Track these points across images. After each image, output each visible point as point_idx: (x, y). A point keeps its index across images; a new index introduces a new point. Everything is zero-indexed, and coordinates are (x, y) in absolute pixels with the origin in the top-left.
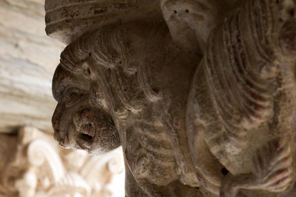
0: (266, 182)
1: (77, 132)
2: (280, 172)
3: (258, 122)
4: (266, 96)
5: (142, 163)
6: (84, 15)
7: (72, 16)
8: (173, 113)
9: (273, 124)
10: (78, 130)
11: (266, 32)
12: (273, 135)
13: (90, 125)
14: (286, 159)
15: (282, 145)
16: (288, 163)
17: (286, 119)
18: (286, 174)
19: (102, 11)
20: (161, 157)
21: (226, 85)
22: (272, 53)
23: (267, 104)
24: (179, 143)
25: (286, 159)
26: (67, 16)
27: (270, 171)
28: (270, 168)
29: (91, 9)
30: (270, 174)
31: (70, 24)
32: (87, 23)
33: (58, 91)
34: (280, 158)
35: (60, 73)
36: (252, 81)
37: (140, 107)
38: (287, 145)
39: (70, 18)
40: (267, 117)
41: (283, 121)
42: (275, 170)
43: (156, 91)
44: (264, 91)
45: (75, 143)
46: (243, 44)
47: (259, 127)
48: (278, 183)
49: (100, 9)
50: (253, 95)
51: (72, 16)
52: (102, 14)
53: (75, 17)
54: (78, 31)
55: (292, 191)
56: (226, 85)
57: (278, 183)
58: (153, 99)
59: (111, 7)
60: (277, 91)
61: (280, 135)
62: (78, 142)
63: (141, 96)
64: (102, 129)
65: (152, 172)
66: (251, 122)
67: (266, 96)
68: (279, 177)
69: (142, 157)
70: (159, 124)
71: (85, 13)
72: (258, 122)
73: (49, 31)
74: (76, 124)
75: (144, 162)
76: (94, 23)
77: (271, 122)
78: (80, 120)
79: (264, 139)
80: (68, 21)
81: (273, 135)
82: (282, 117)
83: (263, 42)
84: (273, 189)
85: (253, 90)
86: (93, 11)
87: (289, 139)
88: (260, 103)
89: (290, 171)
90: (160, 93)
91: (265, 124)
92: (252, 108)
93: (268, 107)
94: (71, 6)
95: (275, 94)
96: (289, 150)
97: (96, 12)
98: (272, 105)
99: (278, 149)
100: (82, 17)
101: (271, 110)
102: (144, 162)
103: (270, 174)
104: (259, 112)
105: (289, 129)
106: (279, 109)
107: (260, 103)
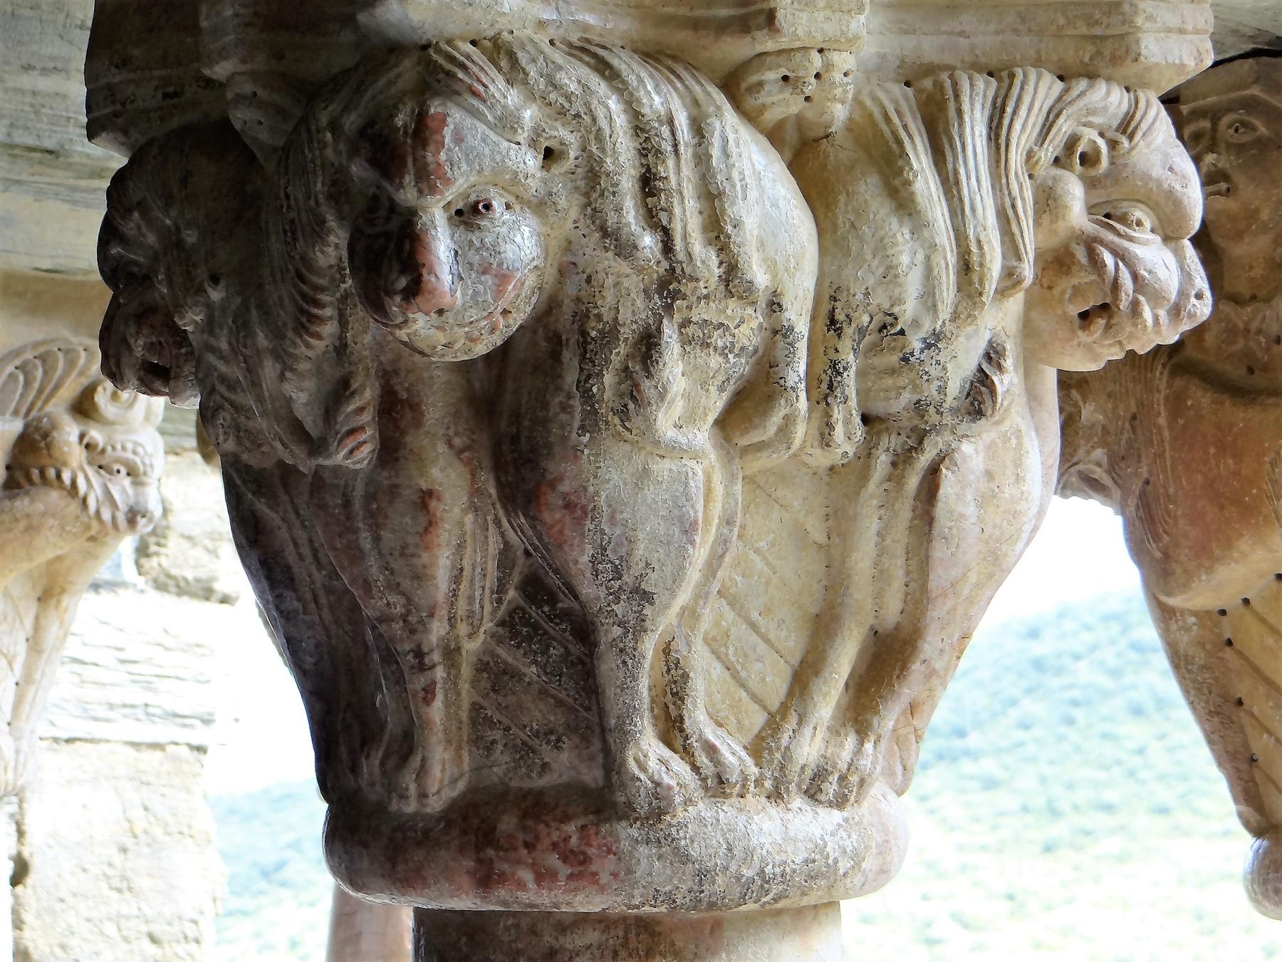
0: (337, 452)
1: (137, 358)
2: (351, 432)
3: (320, 345)
4: (325, 298)
5: (219, 422)
6: (144, 101)
7: (123, 104)
8: (239, 324)
9: (341, 348)
10: (139, 355)
11: (315, 186)
12: (344, 369)
13: (160, 343)
14: (361, 410)
15: (355, 385)
16: (366, 417)
17: (359, 340)
18: (363, 437)
19: (175, 95)
20: (242, 409)
21: (279, 277)
22: (324, 222)
23: (328, 312)
24: (252, 382)
25: (361, 410)
26: (113, 103)
27: (337, 433)
28: (338, 427)
29: (156, 88)
30: (339, 436)
31: (120, 121)
32: (149, 120)
33: (111, 269)
34: (351, 407)
35: (109, 233)
36: (304, 271)
37: (201, 312)
38: (363, 387)
39: (118, 107)
40: (331, 335)
41: (356, 343)
42: (345, 429)
43: (215, 280)
44: (322, 289)
45: (136, 383)
46: (292, 202)
47: (324, 353)
48: (351, 452)
49: (171, 89)
50: (304, 296)
51: (123, 104)
52: (176, 100)
53: (128, 106)
54: (138, 137)
55: (376, 467)
56: (279, 277)
57: (351, 452)
58: (216, 295)
59: (190, 85)
60: (342, 290)
61: (353, 368)
62: (141, 380)
63: (200, 290)
64: (183, 351)
65: (239, 440)
66: (308, 346)
67: (325, 298)
68: (350, 443)
69: (217, 410)
70: (224, 345)
71: (145, 97)
72: (320, 345)
73: (92, 134)
74: (132, 341)
75: (222, 421)
76: (162, 119)
77: (337, 343)
78: (138, 333)
79: (333, 373)
80: (116, 115)
81: (344, 369)
82: (353, 336)
83: (312, 202)
84: (352, 466)
85: (305, 288)
86: (160, 96)
87: (368, 375)
88: (315, 311)
89: (369, 432)
90: (222, 283)
91: (331, 348)
92: (304, 320)
93: (331, 318)
94: (121, 82)
95: (338, 295)
96: (368, 394)
97: (166, 96)
98: (336, 313)
99: (348, 393)
100: (140, 104)
101: (336, 323)
102: (222, 421)
103: (339, 436)
104: (314, 328)
105: (366, 357)
106: (347, 322)
107: (315, 311)
